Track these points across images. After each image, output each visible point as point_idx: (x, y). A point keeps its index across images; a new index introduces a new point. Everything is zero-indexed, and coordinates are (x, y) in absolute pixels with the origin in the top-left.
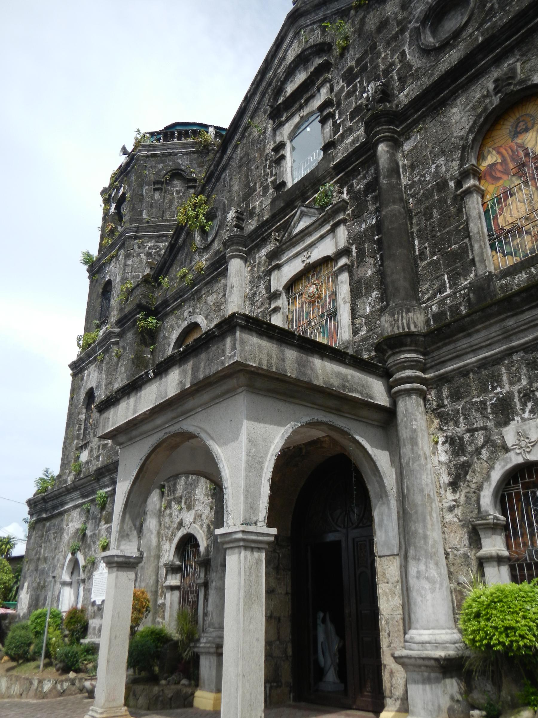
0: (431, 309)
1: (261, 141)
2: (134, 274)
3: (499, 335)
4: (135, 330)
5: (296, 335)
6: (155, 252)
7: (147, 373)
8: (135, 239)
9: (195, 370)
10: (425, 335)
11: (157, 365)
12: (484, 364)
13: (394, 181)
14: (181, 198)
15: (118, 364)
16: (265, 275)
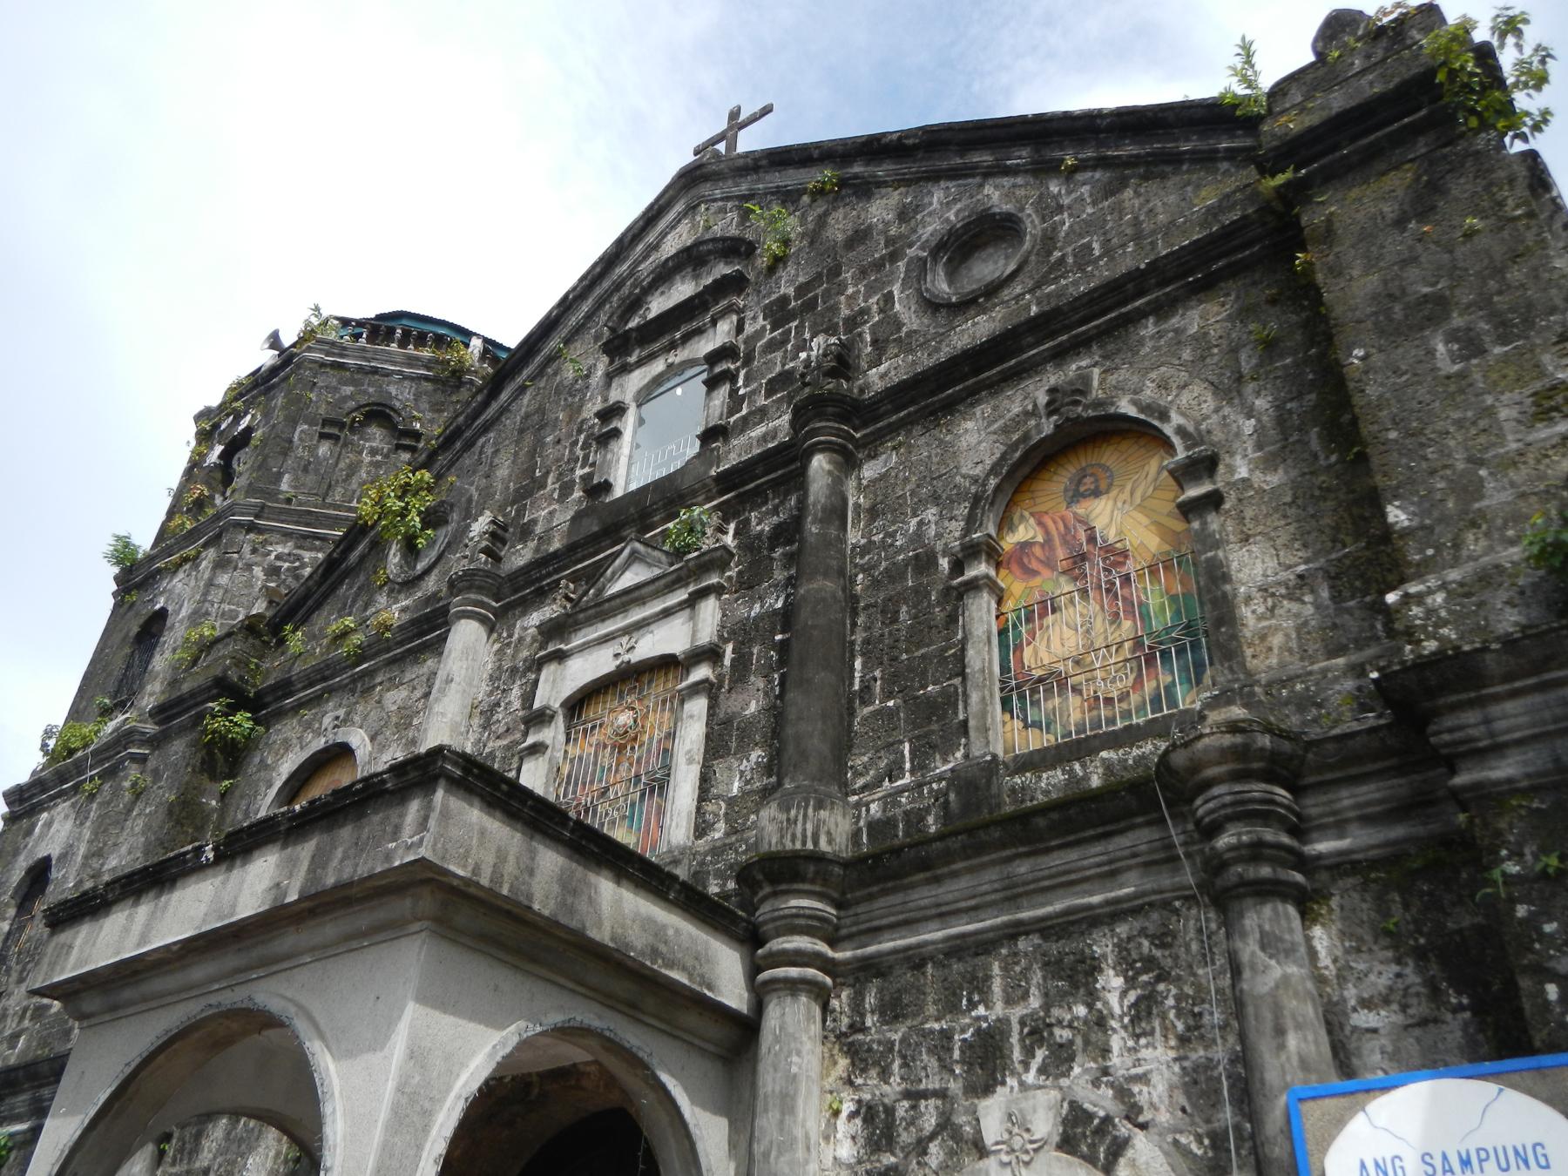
0: (868, 810)
1: (575, 392)
2: (226, 607)
3: (996, 891)
4: (194, 735)
5: (570, 819)
6: (288, 569)
7: (199, 851)
8: (249, 531)
9: (319, 862)
10: (846, 865)
11: (229, 835)
12: (958, 949)
13: (833, 532)
14: (377, 465)
15: (130, 811)
16: (529, 669)
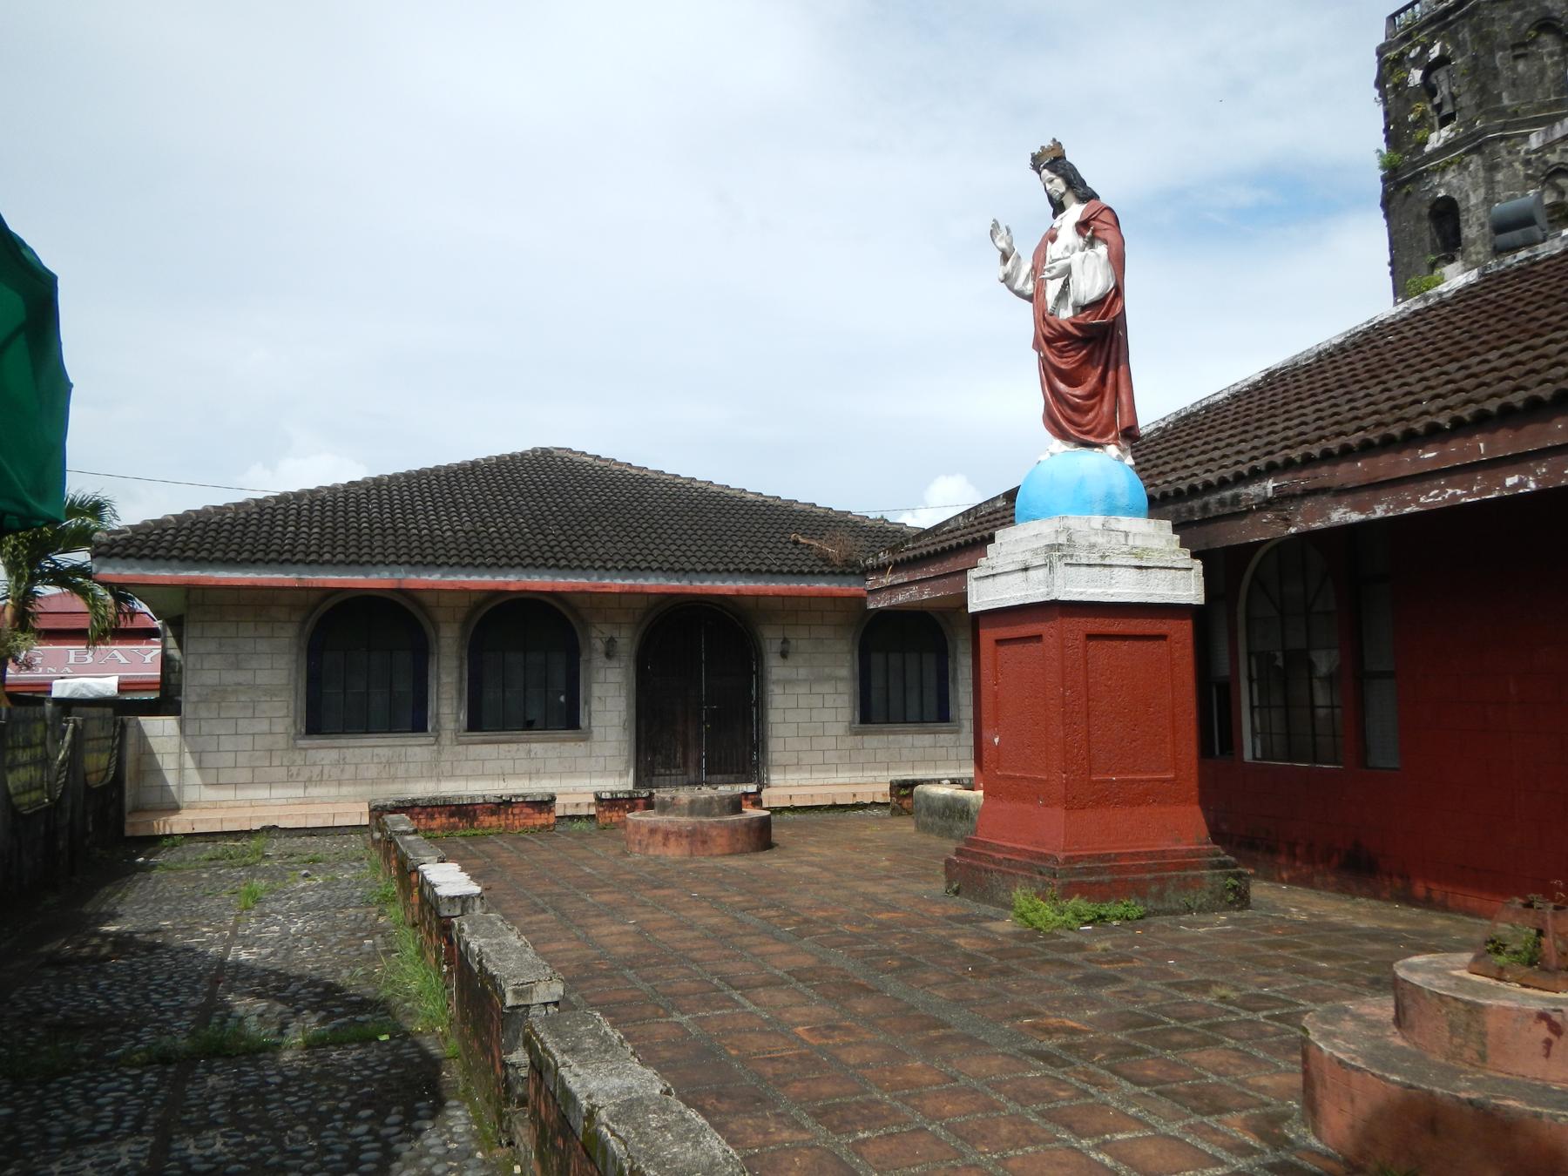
14: (1556, 64)
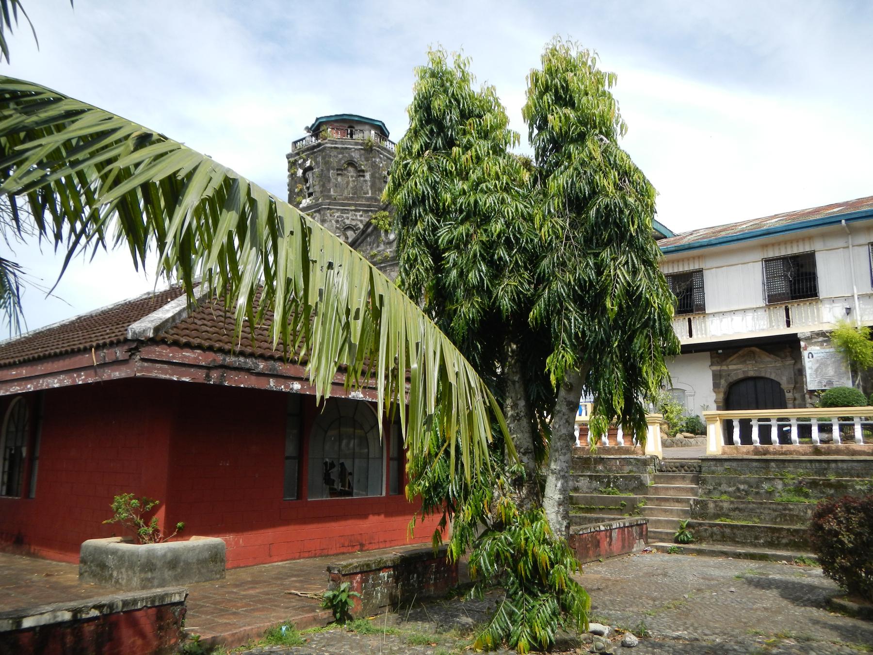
14: (354, 181)
